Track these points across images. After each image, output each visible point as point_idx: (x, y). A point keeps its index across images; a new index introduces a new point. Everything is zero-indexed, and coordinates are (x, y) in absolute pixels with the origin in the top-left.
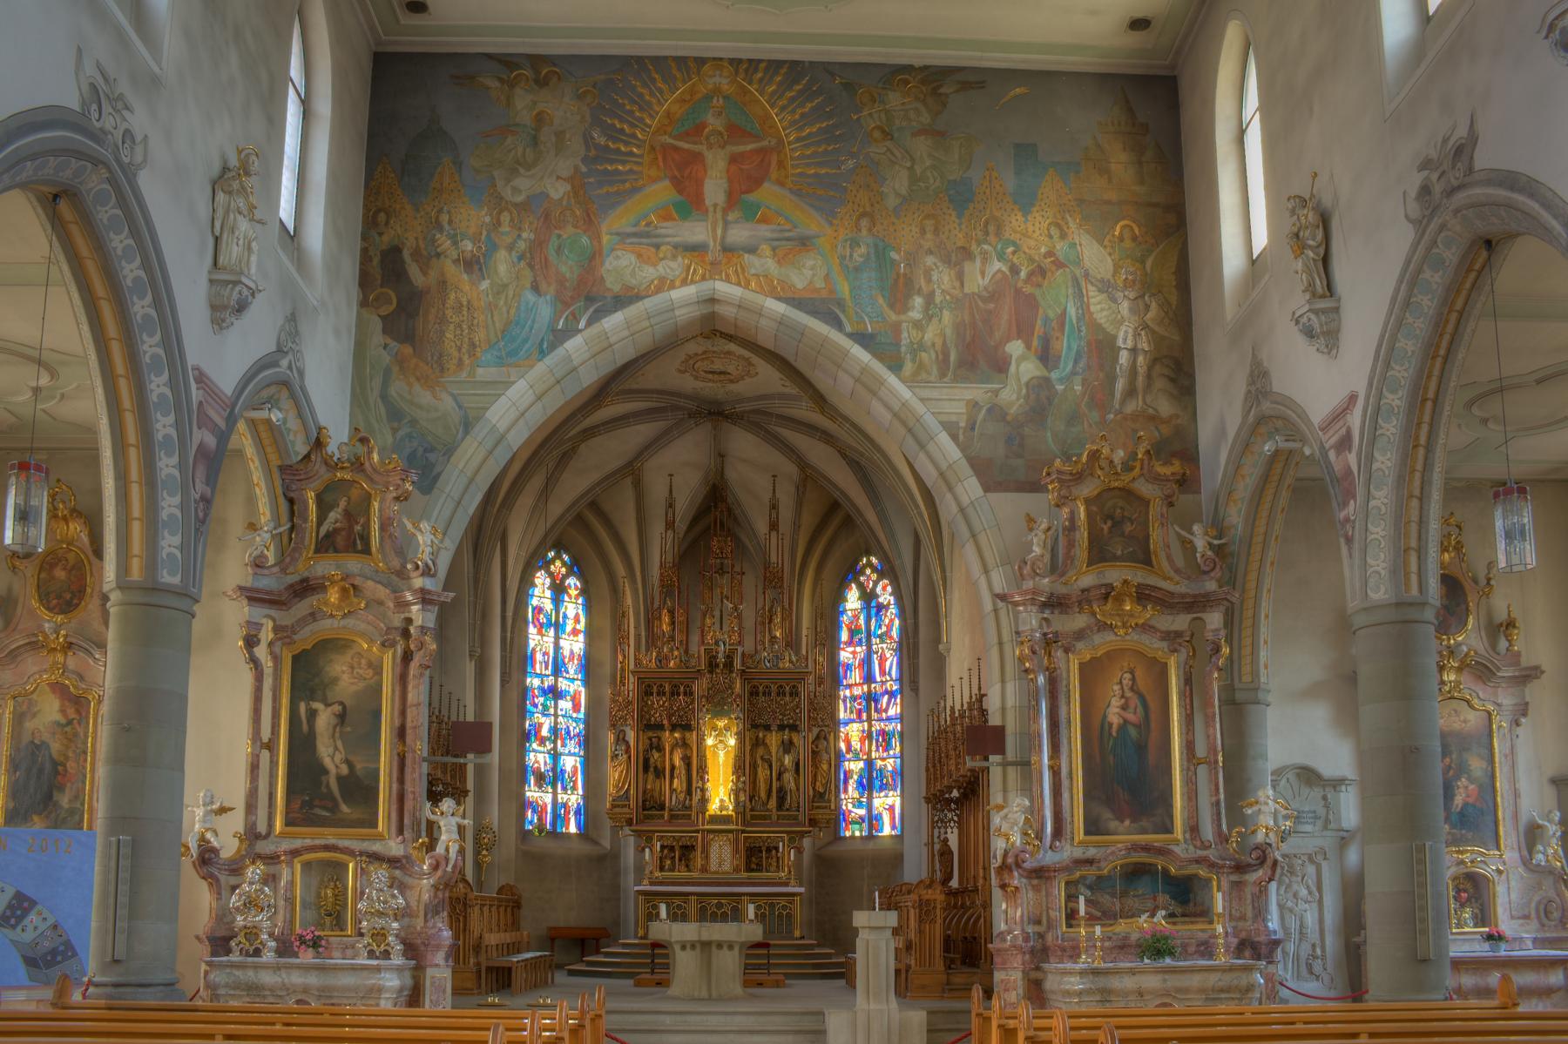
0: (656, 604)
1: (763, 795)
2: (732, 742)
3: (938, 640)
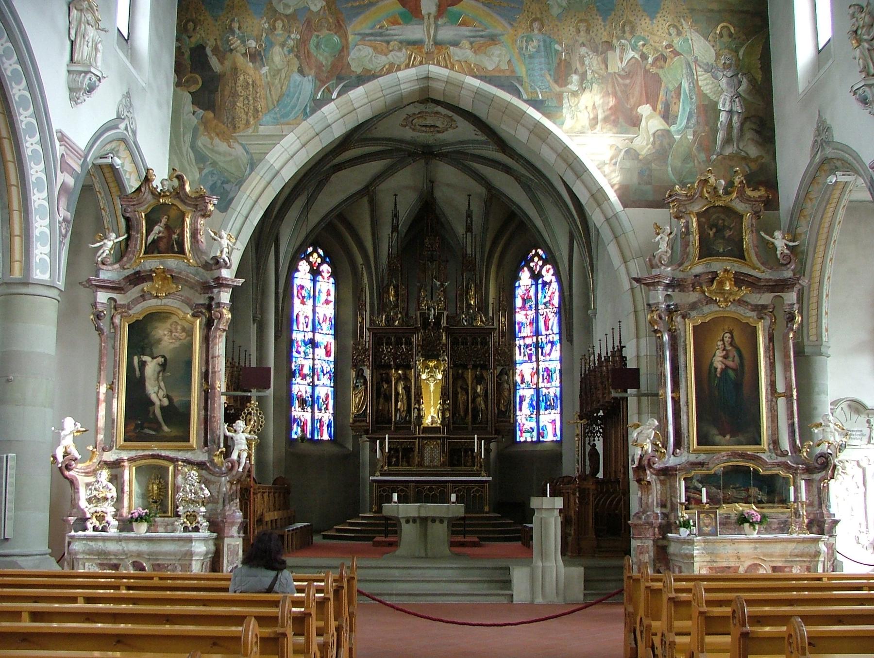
0: (385, 282)
1: (462, 413)
2: (440, 376)
3: (587, 307)
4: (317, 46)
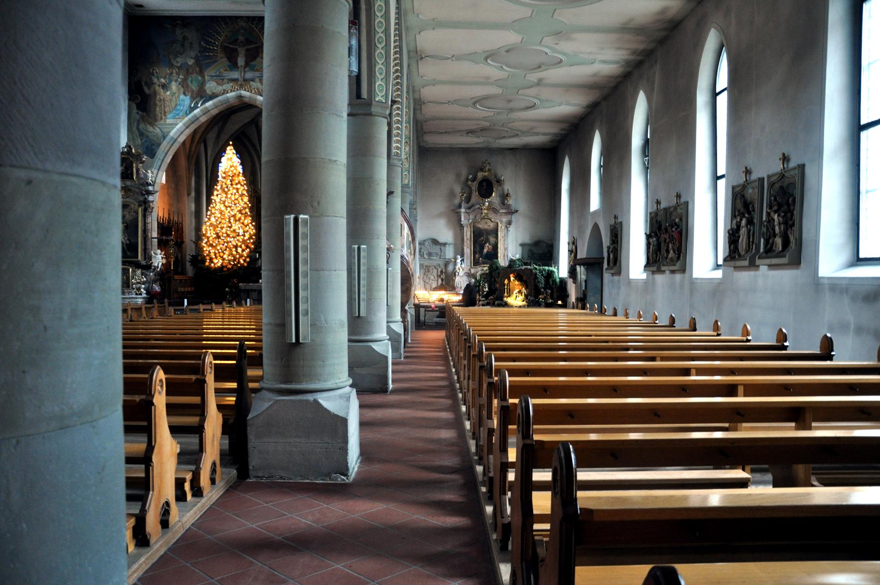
4: (192, 82)
